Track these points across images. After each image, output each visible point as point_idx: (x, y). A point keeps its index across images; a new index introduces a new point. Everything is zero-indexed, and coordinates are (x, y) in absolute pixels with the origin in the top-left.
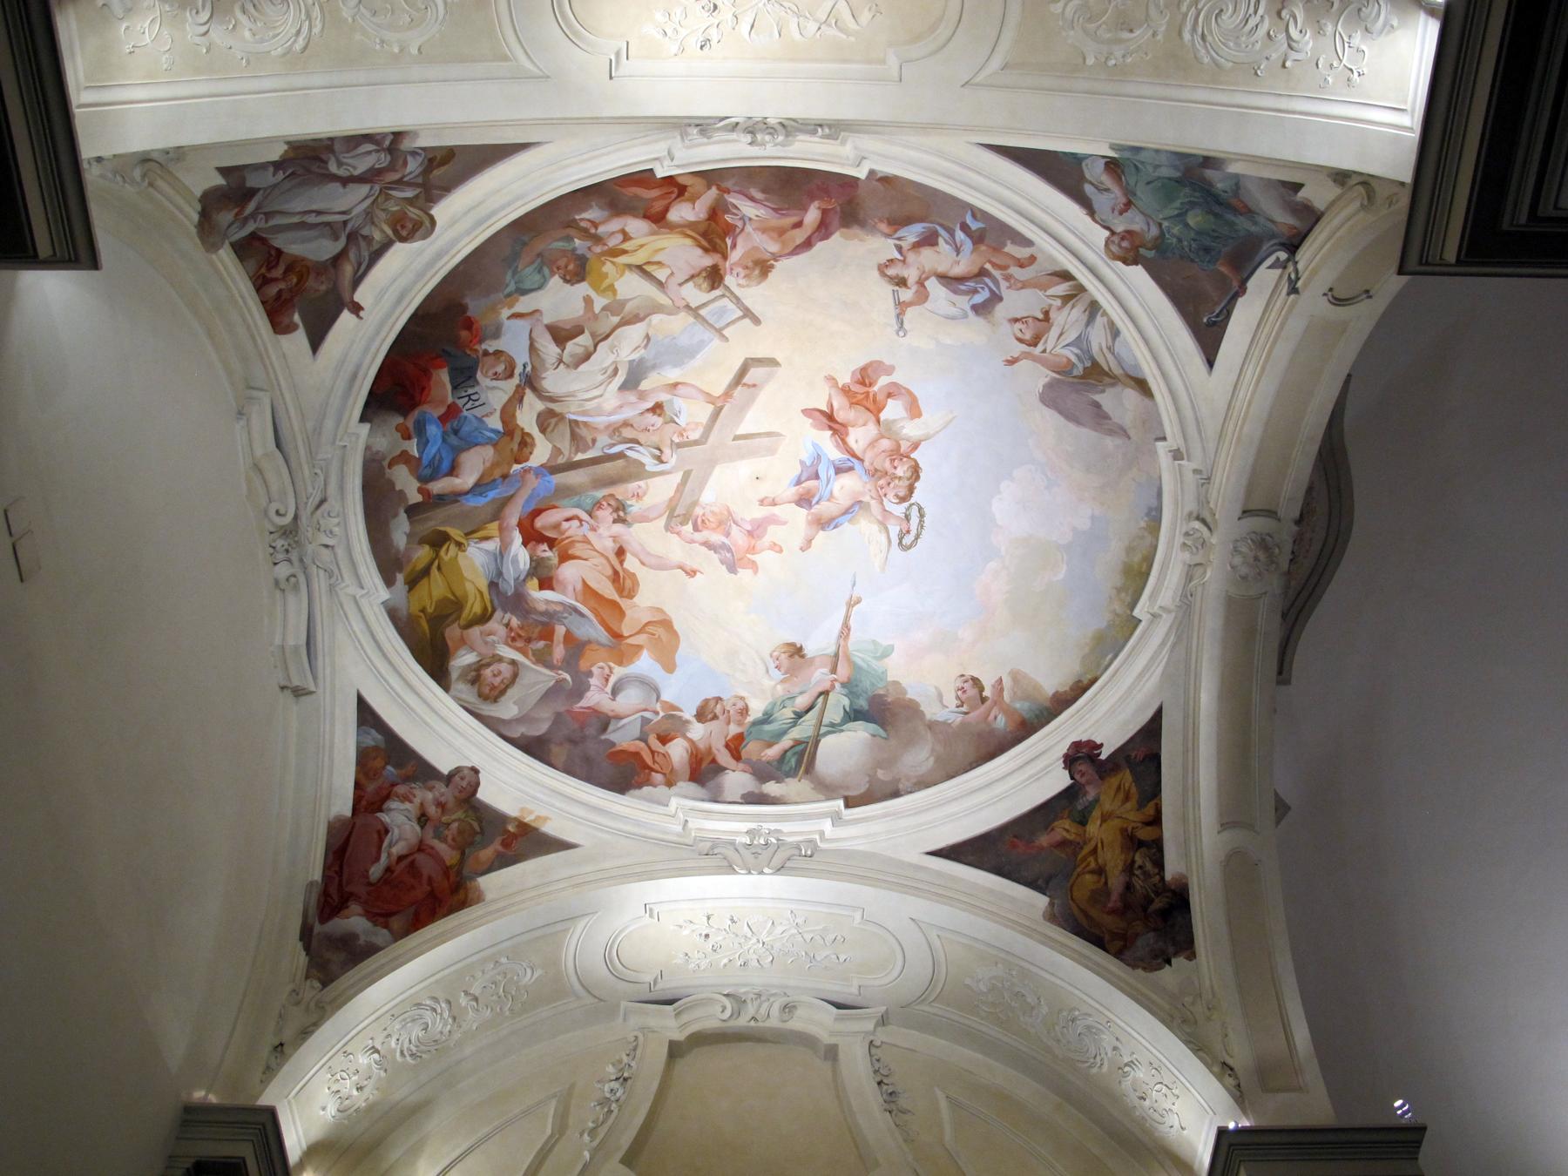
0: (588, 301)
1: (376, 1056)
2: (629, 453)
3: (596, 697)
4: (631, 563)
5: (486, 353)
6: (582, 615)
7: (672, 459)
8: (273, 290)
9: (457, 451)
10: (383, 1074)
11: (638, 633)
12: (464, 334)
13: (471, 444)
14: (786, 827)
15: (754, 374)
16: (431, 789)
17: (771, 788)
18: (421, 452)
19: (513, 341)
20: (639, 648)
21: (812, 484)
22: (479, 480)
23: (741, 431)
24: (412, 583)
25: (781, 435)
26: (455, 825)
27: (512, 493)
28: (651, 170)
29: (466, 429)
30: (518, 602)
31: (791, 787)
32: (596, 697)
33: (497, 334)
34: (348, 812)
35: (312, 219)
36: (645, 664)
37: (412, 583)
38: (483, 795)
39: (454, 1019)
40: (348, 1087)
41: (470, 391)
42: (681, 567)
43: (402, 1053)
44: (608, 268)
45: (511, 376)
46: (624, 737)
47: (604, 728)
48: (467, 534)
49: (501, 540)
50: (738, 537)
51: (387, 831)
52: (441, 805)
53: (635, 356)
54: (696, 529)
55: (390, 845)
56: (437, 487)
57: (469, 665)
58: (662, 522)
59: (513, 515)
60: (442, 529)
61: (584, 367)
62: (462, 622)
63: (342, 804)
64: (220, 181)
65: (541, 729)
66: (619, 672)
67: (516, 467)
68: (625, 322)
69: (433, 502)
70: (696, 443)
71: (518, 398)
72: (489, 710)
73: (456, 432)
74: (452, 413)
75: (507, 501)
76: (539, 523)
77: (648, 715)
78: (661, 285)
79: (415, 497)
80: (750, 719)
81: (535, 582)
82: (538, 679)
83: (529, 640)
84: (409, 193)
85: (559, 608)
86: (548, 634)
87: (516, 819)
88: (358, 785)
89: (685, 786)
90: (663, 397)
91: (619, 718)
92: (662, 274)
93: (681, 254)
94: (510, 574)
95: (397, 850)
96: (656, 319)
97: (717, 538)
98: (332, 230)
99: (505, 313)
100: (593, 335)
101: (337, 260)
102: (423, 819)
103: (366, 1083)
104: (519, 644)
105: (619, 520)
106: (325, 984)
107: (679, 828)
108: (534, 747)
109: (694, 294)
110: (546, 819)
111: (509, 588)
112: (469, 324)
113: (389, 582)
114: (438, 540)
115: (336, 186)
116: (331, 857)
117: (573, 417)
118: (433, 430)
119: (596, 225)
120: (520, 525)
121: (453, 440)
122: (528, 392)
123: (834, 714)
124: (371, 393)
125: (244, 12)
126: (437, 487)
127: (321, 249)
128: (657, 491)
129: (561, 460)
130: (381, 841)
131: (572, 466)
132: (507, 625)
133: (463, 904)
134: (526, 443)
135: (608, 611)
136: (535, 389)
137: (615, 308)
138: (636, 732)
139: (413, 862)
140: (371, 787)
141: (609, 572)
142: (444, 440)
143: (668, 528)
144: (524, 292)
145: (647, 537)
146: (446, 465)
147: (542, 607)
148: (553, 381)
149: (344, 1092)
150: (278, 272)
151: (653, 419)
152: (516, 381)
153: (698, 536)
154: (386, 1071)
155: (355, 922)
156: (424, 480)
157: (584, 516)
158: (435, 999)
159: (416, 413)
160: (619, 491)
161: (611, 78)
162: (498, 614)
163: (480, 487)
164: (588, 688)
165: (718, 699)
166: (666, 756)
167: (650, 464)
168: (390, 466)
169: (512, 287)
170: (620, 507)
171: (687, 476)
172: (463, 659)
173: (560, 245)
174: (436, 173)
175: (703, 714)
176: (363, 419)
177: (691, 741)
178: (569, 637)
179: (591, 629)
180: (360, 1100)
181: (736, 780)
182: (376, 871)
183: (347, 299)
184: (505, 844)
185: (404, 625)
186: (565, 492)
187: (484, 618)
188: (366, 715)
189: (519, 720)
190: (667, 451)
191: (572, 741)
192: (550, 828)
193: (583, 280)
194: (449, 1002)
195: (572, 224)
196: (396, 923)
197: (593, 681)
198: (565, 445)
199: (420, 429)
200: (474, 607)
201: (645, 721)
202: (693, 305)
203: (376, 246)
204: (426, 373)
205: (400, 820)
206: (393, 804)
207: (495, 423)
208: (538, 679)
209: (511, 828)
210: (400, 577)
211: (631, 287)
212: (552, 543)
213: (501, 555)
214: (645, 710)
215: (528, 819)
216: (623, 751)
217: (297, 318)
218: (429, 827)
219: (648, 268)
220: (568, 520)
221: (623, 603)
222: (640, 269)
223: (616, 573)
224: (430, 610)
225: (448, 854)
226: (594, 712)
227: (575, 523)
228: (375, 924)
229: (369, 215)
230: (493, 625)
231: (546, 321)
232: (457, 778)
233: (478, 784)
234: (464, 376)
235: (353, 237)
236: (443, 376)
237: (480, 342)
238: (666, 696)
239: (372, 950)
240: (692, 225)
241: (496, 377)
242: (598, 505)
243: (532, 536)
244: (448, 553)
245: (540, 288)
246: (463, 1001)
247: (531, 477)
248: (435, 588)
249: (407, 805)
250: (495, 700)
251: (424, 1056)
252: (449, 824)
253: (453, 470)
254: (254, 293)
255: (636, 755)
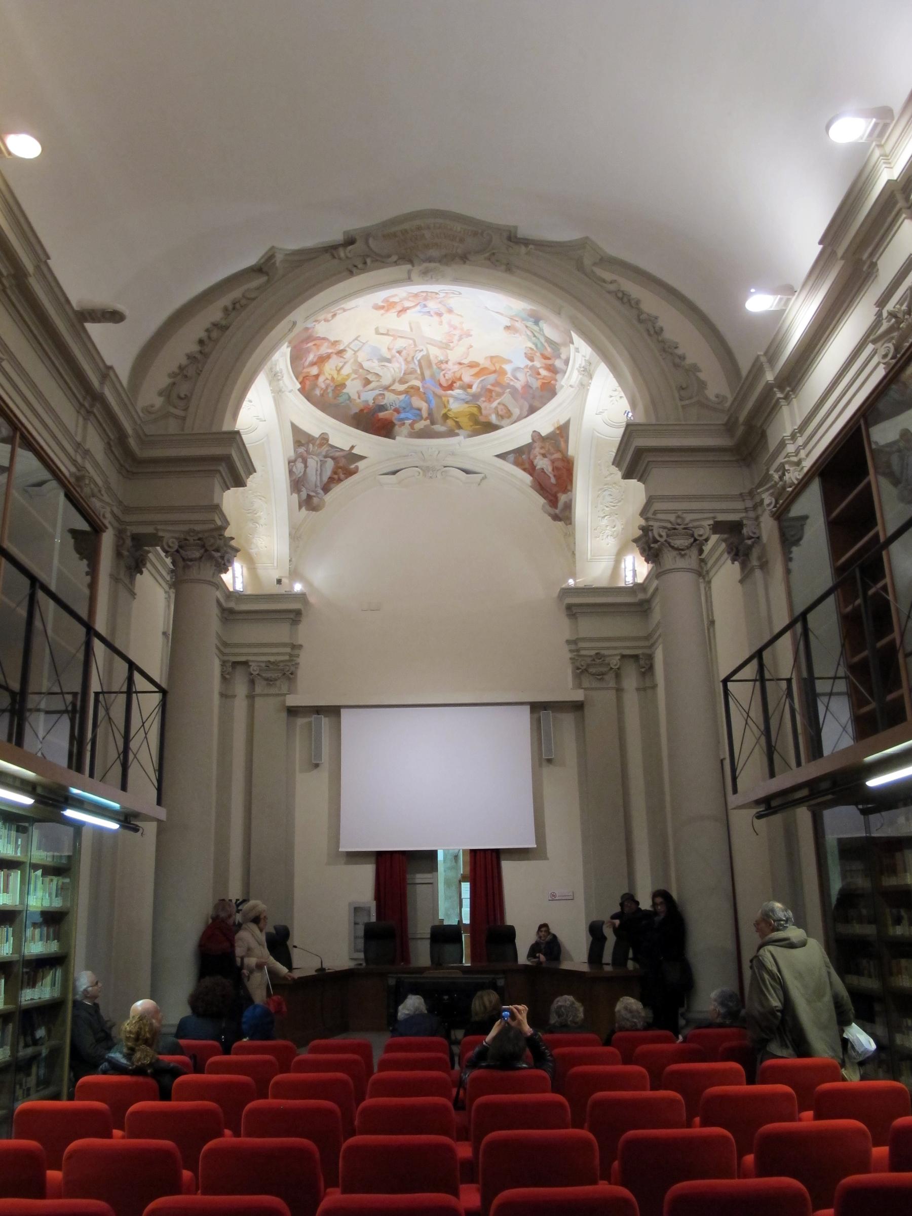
0: (353, 380)
1: (606, 518)
2: (418, 358)
3: (518, 385)
4: (466, 361)
5: (374, 403)
6: (484, 380)
7: (420, 347)
8: (342, 476)
9: (412, 408)
10: (616, 516)
11: (494, 365)
12: (365, 411)
13: (410, 404)
14: (577, 366)
15: (382, 331)
16: (535, 448)
17: (563, 356)
18: (410, 419)
19: (369, 397)
20: (501, 367)
21: (432, 313)
22: (423, 400)
23: (409, 330)
24: (460, 427)
25: (410, 324)
26: (550, 447)
27: (432, 393)
28: (299, 390)
29: (404, 405)
30: (476, 397)
31: (563, 350)
32: (518, 385)
33: (367, 401)
34: (531, 478)
35: (319, 472)
36: (508, 368)
37: (460, 427)
38: (543, 434)
39: (615, 483)
40: (609, 531)
41: (388, 405)
42: (469, 349)
43: (614, 506)
44: (339, 379)
45: (383, 394)
46: (536, 384)
47: (531, 387)
48: (445, 407)
49: (450, 397)
50: (457, 332)
51: (543, 469)
52: (542, 448)
53: (377, 362)
54: (452, 342)
55: (548, 470)
56: (425, 414)
57: (496, 417)
58: (448, 351)
59: (440, 392)
60: (441, 415)
61: (381, 374)
62: (479, 414)
63: (528, 478)
64: (303, 509)
65: (526, 406)
66: (509, 375)
67: (421, 390)
68: (362, 367)
69: (431, 416)
70: (414, 342)
71: (393, 391)
72: (515, 417)
73: (404, 408)
74: (397, 411)
75: (435, 394)
76: (444, 384)
77: (528, 374)
78: (345, 363)
79: (428, 422)
80: (535, 349)
81: (469, 390)
82: (506, 398)
83: (491, 397)
84: (311, 446)
85: (480, 385)
86: (490, 391)
87: (555, 429)
88: (524, 470)
89: (558, 377)
90: (394, 352)
91: (528, 382)
92: (341, 365)
93: (329, 368)
94: (463, 396)
95: (550, 469)
96: (360, 360)
97: (456, 338)
98: (323, 463)
99: (358, 401)
100: (367, 374)
101: (333, 458)
102: (544, 456)
103: (614, 524)
104: (492, 400)
105: (447, 362)
106: (570, 524)
107: (572, 389)
108: (532, 410)
109: (349, 354)
110: (558, 421)
111: (469, 398)
112: (362, 410)
113: (457, 435)
114: (446, 417)
115: (308, 470)
116: (541, 492)
117: (402, 374)
118: (402, 416)
119: (322, 389)
120: (445, 390)
121: (407, 409)
122: (390, 388)
123: (536, 328)
124: (385, 436)
125: (256, 514)
126: (425, 414)
127: (330, 464)
128: (435, 353)
129: (420, 377)
130: (545, 473)
131: (422, 374)
132: (484, 401)
133: (573, 464)
134: (412, 387)
135: (482, 372)
136: (389, 386)
137: (355, 372)
138: (535, 380)
139: (556, 467)
140: (527, 466)
141: (468, 368)
142: (408, 412)
143: (451, 350)
144: (350, 397)
145: (455, 355)
146: (417, 412)
147: (479, 390)
148: (386, 381)
149: (610, 533)
150: (336, 477)
151: (404, 353)
152: (386, 392)
153: (455, 341)
154: (617, 514)
155: (563, 498)
156: (421, 418)
157: (444, 372)
158: (601, 489)
159: (396, 422)
160: (434, 361)
161: (265, 421)
162: (479, 403)
163: (427, 401)
164: (513, 385)
165: (525, 353)
166: (545, 376)
167: (424, 353)
168: (413, 429)
169: (348, 402)
170: (441, 362)
171: (428, 343)
172: (493, 419)
173: (330, 395)
174: (303, 442)
175: (531, 360)
176: (394, 438)
177: (541, 367)
178: (493, 385)
179: (492, 378)
180: (619, 527)
181: (558, 363)
182: (553, 480)
183: (347, 452)
184: (562, 437)
185: (475, 433)
186: (433, 376)
187: (479, 408)
188: (502, 456)
189: (521, 409)
190: (417, 349)
191: (534, 397)
192: (562, 422)
193: (345, 384)
194: (606, 484)
195: (322, 395)
196: (569, 488)
197: (512, 383)
198: (413, 376)
199: (401, 420)
200: (475, 410)
201: (530, 375)
202: (353, 352)
203: (330, 448)
204: (379, 420)
205: (542, 463)
206: (535, 462)
207: (402, 397)
208: (506, 398)
209: (558, 432)
210: (457, 431)
211: (346, 370)
212: (453, 382)
213: (456, 399)
214: (526, 374)
215: (556, 426)
216: (541, 386)
217: (353, 466)
218: (548, 455)
219: (338, 368)
220: (445, 377)
221: (481, 366)
222: (339, 371)
223: (469, 366)
224: (471, 424)
225: (557, 455)
226: (523, 387)
227: (446, 375)
228: (566, 493)
229: (317, 455)
230: (483, 405)
231: (362, 388)
232: (535, 439)
233: (539, 433)
234: (382, 408)
235: (326, 457)
236: (382, 415)
237: (369, 405)
238: (522, 366)
239: (571, 501)
240: (319, 367)
241: (384, 398)
242: (439, 368)
243: (450, 387)
244: (451, 414)
245: (348, 394)
246: (608, 479)
247: (426, 386)
248: (464, 421)
249: (538, 458)
250: (512, 414)
251: (623, 497)
252: (549, 449)
253: (420, 410)
254: (342, 483)
255: (543, 384)
